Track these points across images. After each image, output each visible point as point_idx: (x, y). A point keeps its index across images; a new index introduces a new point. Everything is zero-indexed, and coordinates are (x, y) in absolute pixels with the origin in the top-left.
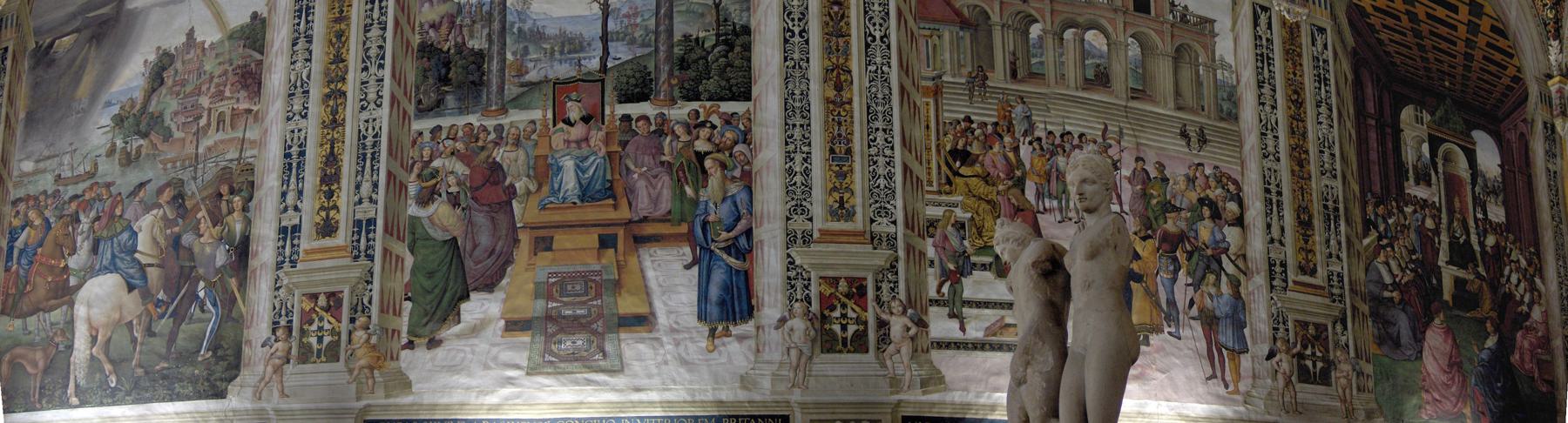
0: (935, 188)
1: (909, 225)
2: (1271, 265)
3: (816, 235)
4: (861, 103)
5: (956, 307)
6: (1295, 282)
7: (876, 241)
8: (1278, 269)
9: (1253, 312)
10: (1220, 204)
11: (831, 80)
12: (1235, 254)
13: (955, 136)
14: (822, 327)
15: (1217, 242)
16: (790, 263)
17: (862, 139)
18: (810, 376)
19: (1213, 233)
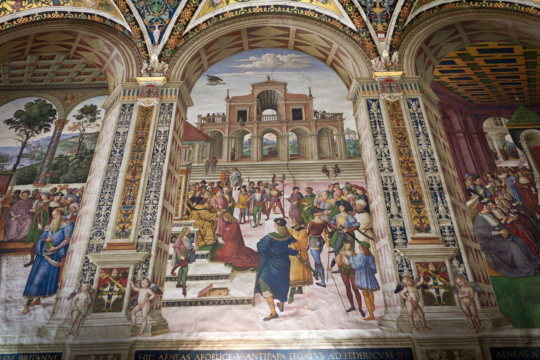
0: (179, 217)
2: (393, 231)
3: (105, 246)
4: (144, 181)
7: (139, 248)
8: (398, 232)
9: (381, 262)
10: (352, 202)
11: (131, 171)
12: (364, 229)
14: (97, 297)
16: (86, 262)
17: (142, 197)
18: (82, 327)
19: (347, 219)
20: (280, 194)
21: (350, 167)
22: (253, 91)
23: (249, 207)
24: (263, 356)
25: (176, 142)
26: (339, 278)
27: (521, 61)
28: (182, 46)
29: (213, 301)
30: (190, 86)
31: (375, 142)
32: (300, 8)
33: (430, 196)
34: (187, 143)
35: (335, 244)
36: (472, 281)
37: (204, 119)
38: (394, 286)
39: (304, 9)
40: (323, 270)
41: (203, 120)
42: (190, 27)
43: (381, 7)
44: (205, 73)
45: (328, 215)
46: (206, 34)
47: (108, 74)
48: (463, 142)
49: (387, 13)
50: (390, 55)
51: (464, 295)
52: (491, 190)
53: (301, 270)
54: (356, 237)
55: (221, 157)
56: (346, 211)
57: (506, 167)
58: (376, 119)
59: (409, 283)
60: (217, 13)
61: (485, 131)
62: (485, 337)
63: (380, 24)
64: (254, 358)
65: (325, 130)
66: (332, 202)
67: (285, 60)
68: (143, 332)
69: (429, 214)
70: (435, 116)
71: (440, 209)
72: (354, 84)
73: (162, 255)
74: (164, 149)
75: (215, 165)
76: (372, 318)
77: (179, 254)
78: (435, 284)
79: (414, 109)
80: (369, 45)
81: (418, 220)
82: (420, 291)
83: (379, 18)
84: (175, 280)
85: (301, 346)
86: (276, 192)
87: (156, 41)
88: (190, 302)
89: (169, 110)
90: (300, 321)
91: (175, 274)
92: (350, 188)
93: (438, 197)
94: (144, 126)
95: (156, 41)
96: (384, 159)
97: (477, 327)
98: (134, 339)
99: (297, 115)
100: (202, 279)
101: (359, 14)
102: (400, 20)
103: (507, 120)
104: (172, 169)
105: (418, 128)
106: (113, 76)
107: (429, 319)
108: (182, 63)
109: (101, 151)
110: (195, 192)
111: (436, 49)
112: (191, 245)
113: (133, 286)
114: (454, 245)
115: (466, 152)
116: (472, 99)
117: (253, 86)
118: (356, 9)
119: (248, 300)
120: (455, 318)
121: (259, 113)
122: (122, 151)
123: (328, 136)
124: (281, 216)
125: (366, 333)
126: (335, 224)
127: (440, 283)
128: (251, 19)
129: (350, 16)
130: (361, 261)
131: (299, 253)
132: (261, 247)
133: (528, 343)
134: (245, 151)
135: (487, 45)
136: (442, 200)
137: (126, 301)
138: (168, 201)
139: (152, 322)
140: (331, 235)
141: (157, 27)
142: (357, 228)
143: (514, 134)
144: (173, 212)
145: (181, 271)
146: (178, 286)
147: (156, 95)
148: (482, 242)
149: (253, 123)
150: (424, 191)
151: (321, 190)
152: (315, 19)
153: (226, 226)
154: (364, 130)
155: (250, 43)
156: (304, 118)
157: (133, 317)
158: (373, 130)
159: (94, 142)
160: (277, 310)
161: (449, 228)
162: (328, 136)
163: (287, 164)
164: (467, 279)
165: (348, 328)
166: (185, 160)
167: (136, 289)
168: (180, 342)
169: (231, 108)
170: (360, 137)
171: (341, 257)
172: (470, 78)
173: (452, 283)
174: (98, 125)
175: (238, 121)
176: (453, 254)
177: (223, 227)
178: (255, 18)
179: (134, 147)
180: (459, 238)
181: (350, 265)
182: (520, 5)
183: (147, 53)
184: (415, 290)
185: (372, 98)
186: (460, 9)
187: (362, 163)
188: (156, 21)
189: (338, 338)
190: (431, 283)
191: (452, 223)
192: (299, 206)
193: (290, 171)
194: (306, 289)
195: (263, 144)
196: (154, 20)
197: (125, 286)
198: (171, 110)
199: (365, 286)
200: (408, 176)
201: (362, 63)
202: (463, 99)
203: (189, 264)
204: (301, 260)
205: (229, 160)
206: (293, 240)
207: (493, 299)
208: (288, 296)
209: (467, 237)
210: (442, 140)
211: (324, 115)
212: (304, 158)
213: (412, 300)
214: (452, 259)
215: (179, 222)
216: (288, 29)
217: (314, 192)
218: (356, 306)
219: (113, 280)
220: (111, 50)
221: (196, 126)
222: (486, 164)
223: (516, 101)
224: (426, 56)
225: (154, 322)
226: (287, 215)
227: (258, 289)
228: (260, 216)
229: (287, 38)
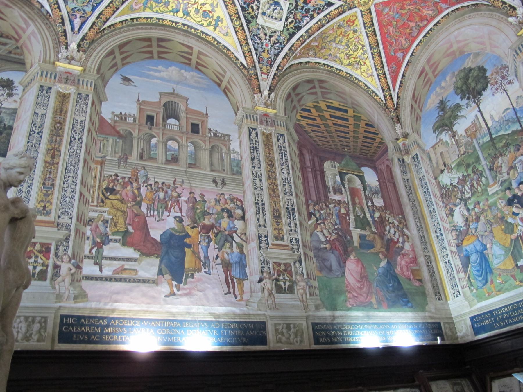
0: (95, 204)
1: (79, 220)
2: (260, 237)
6: (273, 244)
7: (60, 227)
8: (263, 239)
9: (250, 260)
10: (233, 211)
11: (50, 153)
13: (109, 182)
17: (61, 180)
19: (229, 224)
20: (179, 196)
23: (154, 203)
24: (164, 323)
25: (92, 134)
26: (220, 268)
27: (351, 121)
28: (98, 39)
29: (125, 279)
30: (105, 82)
31: (252, 164)
32: (203, 33)
33: (286, 214)
34: (102, 136)
35: (219, 242)
37: (117, 116)
39: (207, 34)
40: (210, 262)
41: (116, 117)
42: (108, 24)
43: (268, 53)
44: (119, 72)
45: (215, 218)
46: (120, 33)
47: (25, 50)
48: (310, 175)
50: (269, 94)
52: (324, 215)
53: (194, 260)
54: (234, 239)
55: (131, 154)
57: (334, 200)
58: (254, 145)
59: (268, 276)
60: (133, 16)
61: (325, 170)
62: (309, 316)
63: (265, 67)
64: (157, 325)
66: (219, 208)
67: (188, 77)
68: (67, 299)
69: (284, 228)
71: (292, 224)
72: (241, 112)
73: (81, 236)
74: (81, 138)
75: (126, 161)
76: (242, 300)
77: (95, 236)
78: (284, 279)
80: (254, 81)
81: (277, 231)
82: (274, 282)
83: (265, 62)
84: (92, 258)
85: (192, 318)
87: (76, 29)
88: (106, 278)
89: (85, 100)
90: (192, 300)
91: (92, 253)
92: (233, 200)
94: (61, 111)
95: (76, 29)
98: (58, 305)
99: (195, 129)
100: (115, 260)
101: (252, 55)
103: (338, 165)
104: (88, 159)
105: (282, 158)
106: (30, 54)
108: (98, 57)
109: (19, 128)
110: (109, 183)
111: (300, 96)
112: (105, 230)
113: (55, 260)
114: (297, 252)
115: (311, 184)
116: (319, 143)
117: (161, 94)
118: (250, 49)
121: (164, 120)
122: (40, 132)
124: (179, 214)
125: (237, 311)
126: (220, 227)
128: (160, 29)
129: (244, 53)
133: (332, 320)
135: (332, 103)
136: (293, 218)
137: (50, 272)
138: (85, 187)
140: (217, 235)
141: (78, 17)
142: (235, 232)
143: (342, 175)
144: (90, 199)
145: (98, 251)
146: (96, 264)
147: (73, 83)
148: (315, 251)
149: (159, 129)
150: (283, 209)
152: (214, 45)
153: (135, 217)
154: (245, 153)
155: (159, 52)
156: (201, 133)
157: (57, 287)
158: (252, 154)
159: (12, 118)
160: (175, 290)
161: (296, 239)
165: (225, 306)
166: (100, 152)
167: (58, 263)
168: (99, 310)
169: (141, 110)
170: (242, 158)
171: (223, 253)
172: (319, 127)
173: (294, 279)
174: (15, 101)
175: (147, 124)
178: (165, 30)
179: (53, 131)
180: (301, 247)
181: (229, 260)
182: (355, 78)
183: (66, 39)
184: (271, 281)
185: (253, 127)
186: (318, 69)
187: (242, 179)
188: (78, 10)
189: (218, 313)
190: (281, 278)
194: (196, 275)
195: (167, 150)
196: (76, 9)
197: (48, 259)
198: (87, 101)
199: (238, 276)
200: (273, 196)
201: (247, 94)
202: (313, 142)
203: (104, 246)
204: (193, 252)
206: (188, 236)
207: (317, 291)
208: (183, 280)
209: (306, 247)
210: (298, 172)
212: (199, 168)
213: (268, 289)
215: (95, 208)
216: (191, 48)
218: (232, 291)
219: (37, 253)
220: (28, 26)
221: (109, 121)
222: (323, 195)
223: (345, 151)
224: (292, 101)
225: (76, 292)
226: (184, 214)
227: (160, 272)
229: (190, 57)
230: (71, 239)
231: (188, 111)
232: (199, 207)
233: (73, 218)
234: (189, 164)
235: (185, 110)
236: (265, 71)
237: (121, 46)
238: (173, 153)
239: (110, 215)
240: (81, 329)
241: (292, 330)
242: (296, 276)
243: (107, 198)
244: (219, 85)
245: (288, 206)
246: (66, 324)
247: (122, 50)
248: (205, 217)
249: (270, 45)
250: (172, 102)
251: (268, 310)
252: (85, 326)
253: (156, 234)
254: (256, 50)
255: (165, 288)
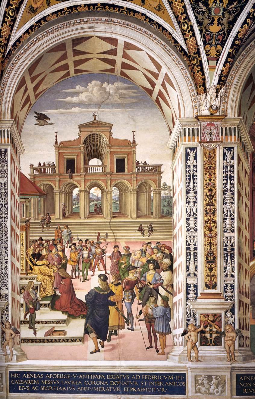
2: (188, 287)
5: (32, 323)
6: (202, 294)
8: (192, 288)
15: (156, 281)
19: (154, 276)
20: (103, 252)
21: (162, 227)
22: (80, 135)
31: (187, 199)
33: (222, 256)
36: (237, 328)
37: (35, 169)
38: (181, 331)
41: (35, 171)
45: (140, 272)
49: (224, 33)
51: (229, 339)
54: (160, 292)
56: (155, 269)
58: (192, 173)
59: (193, 329)
63: (213, 48)
65: (144, 185)
66: (144, 260)
67: (111, 92)
69: (218, 274)
70: (245, 170)
71: (228, 268)
73: (16, 304)
75: (49, 222)
76: (163, 353)
77: (28, 303)
78: (211, 330)
79: (228, 161)
81: (209, 278)
82: (199, 335)
84: (27, 323)
86: (100, 250)
88: (39, 340)
91: (27, 319)
93: (229, 257)
96: (192, 218)
97: (232, 361)
99: (120, 165)
100: (46, 324)
101: (194, 35)
102: (237, 42)
105: (227, 184)
107: (201, 355)
114: (231, 300)
117: (81, 127)
119: (79, 339)
120: (219, 355)
121: (86, 163)
123: (146, 192)
124: (103, 272)
126: (145, 281)
127: (214, 329)
130: (161, 311)
131: (116, 304)
132: (88, 299)
134: (74, 207)
136: (231, 260)
138: (14, 257)
139: (16, 353)
140: (141, 289)
142: (161, 284)
146: (30, 328)
149: (81, 175)
151: (136, 249)
156: (126, 171)
158: (187, 185)
161: (231, 285)
162: (146, 192)
163: (110, 222)
164: (234, 327)
166: (23, 217)
169: (60, 155)
170: (174, 194)
171: (147, 309)
175: (67, 173)
176: (229, 307)
177: (59, 282)
190: (208, 329)
191: (234, 281)
192: (118, 263)
193: (112, 230)
194: (120, 332)
195: (90, 200)
203: (36, 312)
204: (117, 309)
205: (61, 217)
206: (112, 293)
207: (248, 342)
210: (245, 199)
211: (145, 167)
213: (192, 342)
214: (227, 311)
215: (25, 276)
217: (130, 251)
218: (153, 345)
221: (29, 177)
226: (108, 272)
227: (87, 332)
228: (87, 273)
229: (114, 57)
230: (10, 307)
231: (113, 143)
232: (123, 262)
233: (9, 289)
234: (113, 212)
235: (108, 142)
236: (213, 53)
237: (31, 69)
238: (96, 203)
239: (40, 281)
240: (24, 382)
241: (214, 381)
242: (225, 326)
243: (34, 265)
244: (150, 92)
245: (226, 246)
246: (13, 378)
247: (33, 76)
248: (129, 272)
249: (221, 9)
250: (93, 134)
251: (190, 362)
252: (27, 379)
253: (81, 295)
254: (199, 23)
255: (91, 344)
